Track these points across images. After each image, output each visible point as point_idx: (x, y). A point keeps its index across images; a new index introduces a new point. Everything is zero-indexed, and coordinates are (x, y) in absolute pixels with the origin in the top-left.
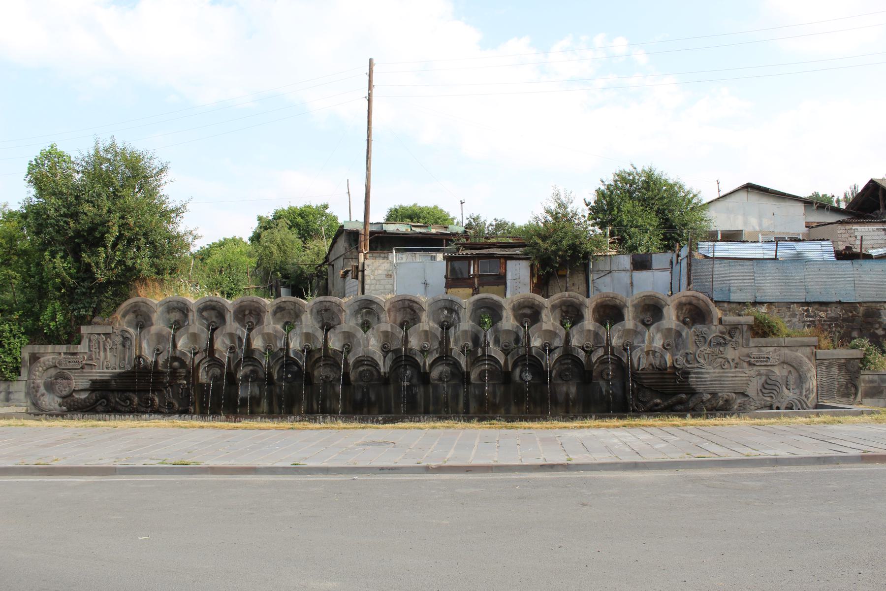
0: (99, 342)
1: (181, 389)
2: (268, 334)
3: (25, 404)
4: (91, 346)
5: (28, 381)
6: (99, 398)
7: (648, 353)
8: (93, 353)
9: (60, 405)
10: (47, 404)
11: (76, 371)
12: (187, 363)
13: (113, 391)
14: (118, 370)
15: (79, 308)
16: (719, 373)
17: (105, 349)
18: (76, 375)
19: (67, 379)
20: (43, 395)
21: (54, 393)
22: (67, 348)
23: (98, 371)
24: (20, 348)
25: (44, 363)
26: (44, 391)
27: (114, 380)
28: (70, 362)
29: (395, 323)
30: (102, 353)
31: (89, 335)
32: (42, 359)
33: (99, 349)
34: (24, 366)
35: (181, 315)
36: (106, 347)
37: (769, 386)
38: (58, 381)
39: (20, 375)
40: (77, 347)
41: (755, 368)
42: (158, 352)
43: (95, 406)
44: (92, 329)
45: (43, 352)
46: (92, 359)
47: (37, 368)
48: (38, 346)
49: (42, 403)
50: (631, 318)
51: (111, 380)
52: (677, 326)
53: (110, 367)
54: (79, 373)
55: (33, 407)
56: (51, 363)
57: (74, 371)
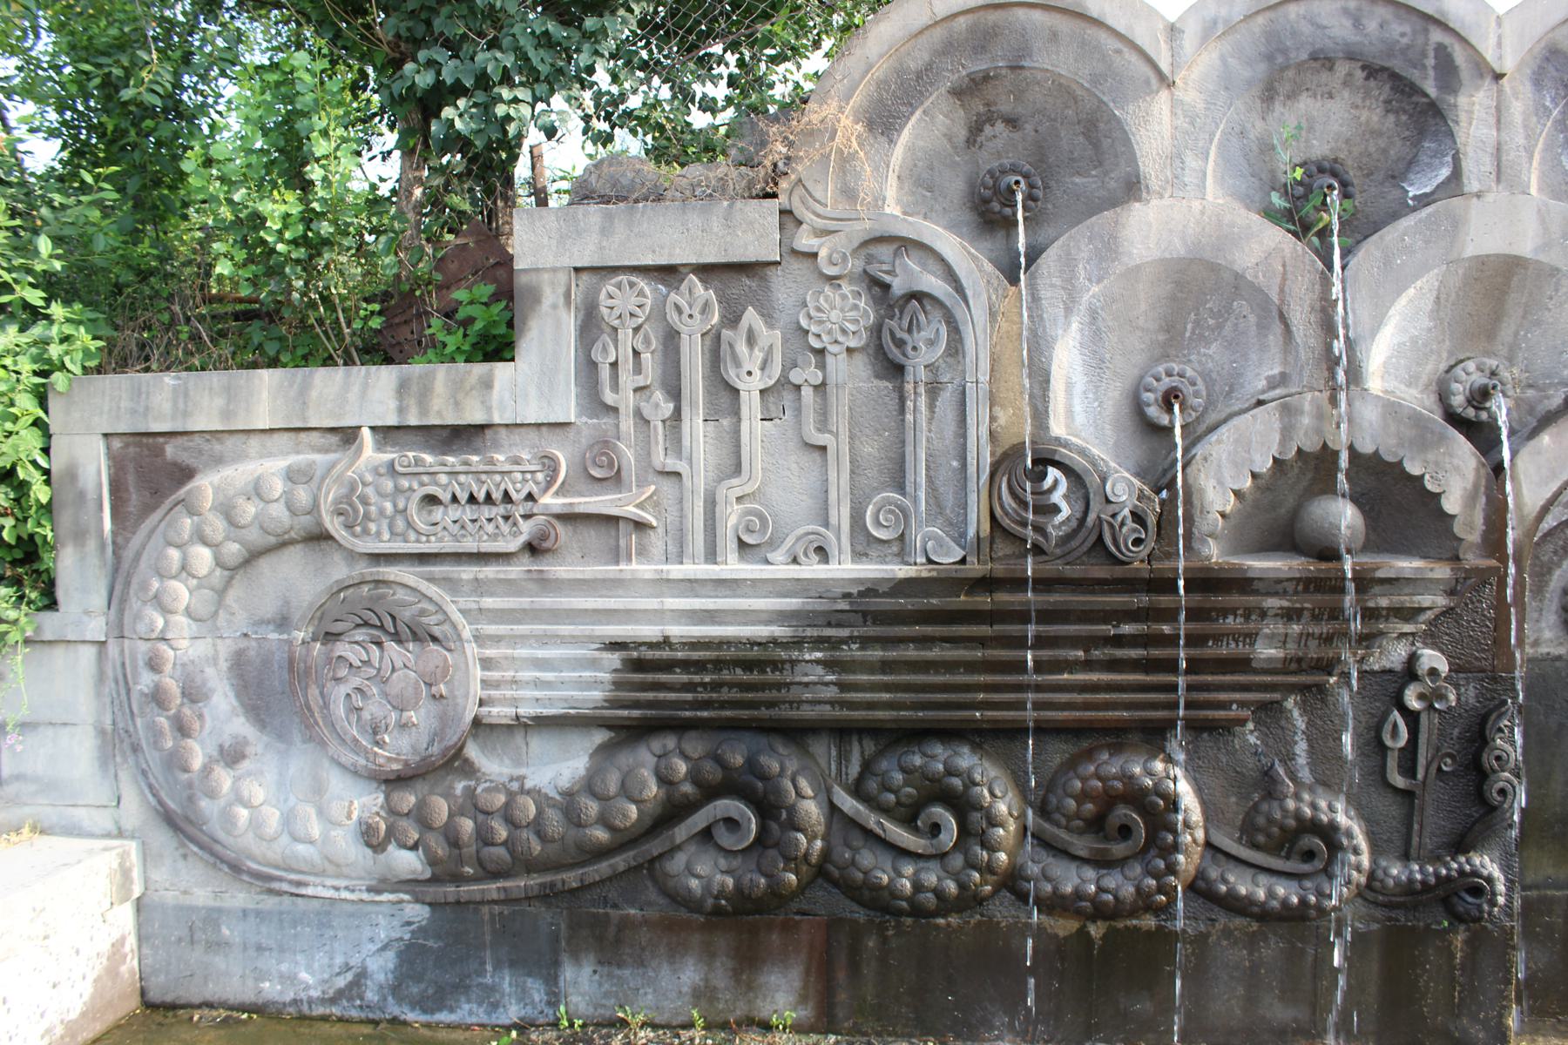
0: (671, 338)
1: (1412, 718)
3: (104, 820)
4: (605, 373)
5: (113, 649)
6: (687, 788)
8: (627, 424)
9: (373, 840)
10: (272, 819)
11: (489, 571)
12: (1451, 505)
13: (796, 733)
14: (845, 569)
15: (483, 81)
17: (725, 394)
18: (489, 602)
19: (419, 635)
20: (232, 755)
21: (313, 738)
22: (402, 388)
23: (676, 571)
24: (42, 399)
25: (227, 512)
26: (241, 726)
27: (818, 642)
28: (432, 500)
30: (697, 429)
31: (585, 277)
32: (206, 485)
33: (675, 394)
34: (79, 536)
35: (1373, 115)
36: (731, 374)
38: (342, 649)
39: (52, 604)
40: (487, 384)
43: (655, 847)
44: (605, 231)
45: (217, 426)
46: (615, 479)
47: (174, 554)
48: (169, 379)
49: (228, 819)
51: (798, 643)
53: (773, 544)
54: (510, 586)
55: (162, 838)
56: (278, 511)
57: (467, 572)
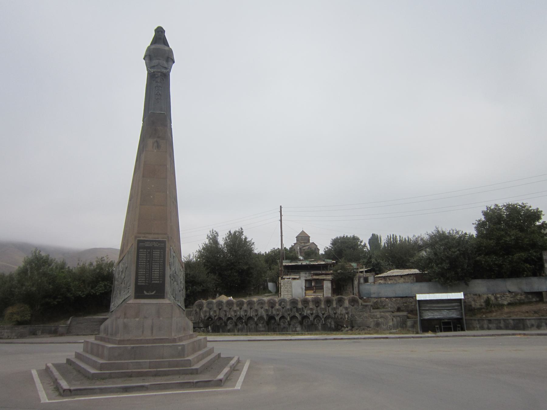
2: (235, 310)
7: (340, 314)
16: (361, 320)
29: (269, 306)
37: (378, 325)
41: (373, 319)
42: (205, 317)
50: (335, 304)
52: (349, 306)
